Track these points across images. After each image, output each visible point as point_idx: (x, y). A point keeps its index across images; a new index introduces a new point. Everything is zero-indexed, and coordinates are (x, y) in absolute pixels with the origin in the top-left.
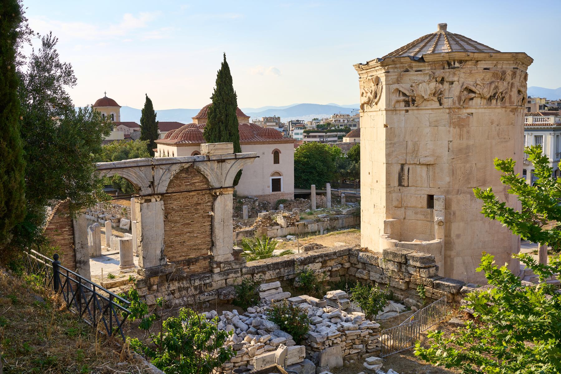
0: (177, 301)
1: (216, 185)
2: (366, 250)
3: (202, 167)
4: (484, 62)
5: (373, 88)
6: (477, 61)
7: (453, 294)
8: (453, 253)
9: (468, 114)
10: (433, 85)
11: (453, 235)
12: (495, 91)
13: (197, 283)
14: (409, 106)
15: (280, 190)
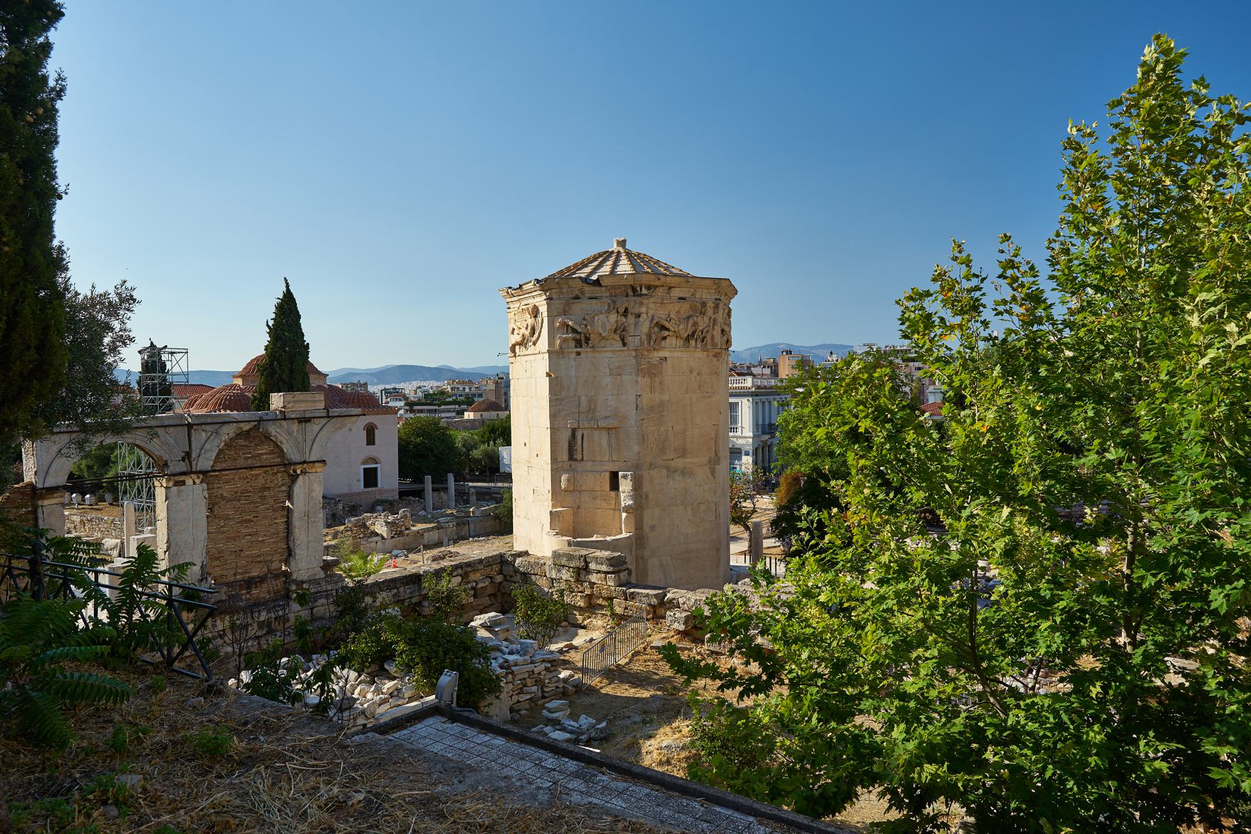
0: (229, 649)
1: (296, 457)
2: (526, 553)
3: (273, 429)
5: (530, 321)
7: (654, 606)
8: (647, 553)
10: (613, 317)
11: (646, 528)
13: (263, 616)
15: (376, 485)
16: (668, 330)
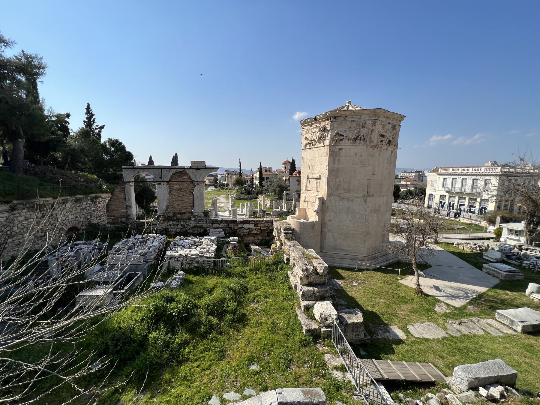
0: (172, 230)
1: (194, 180)
6: (346, 117)
8: (326, 230)
9: (340, 149)
11: (327, 219)
13: (182, 223)
16: (343, 136)
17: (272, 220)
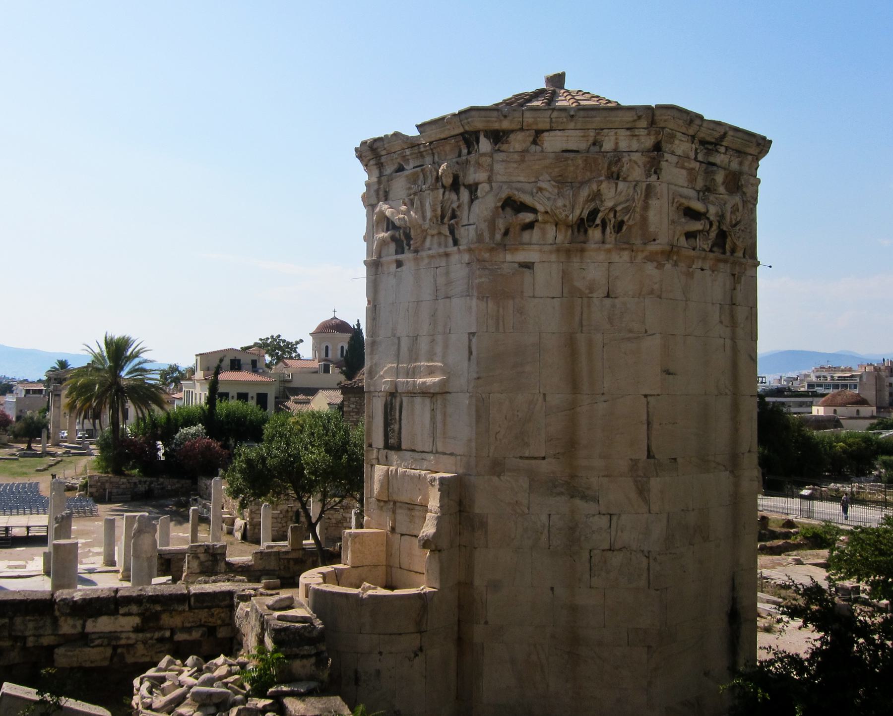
4: (558, 133)
6: (539, 132)
12: (592, 206)
14: (403, 253)
16: (534, 211)
17: (230, 594)
